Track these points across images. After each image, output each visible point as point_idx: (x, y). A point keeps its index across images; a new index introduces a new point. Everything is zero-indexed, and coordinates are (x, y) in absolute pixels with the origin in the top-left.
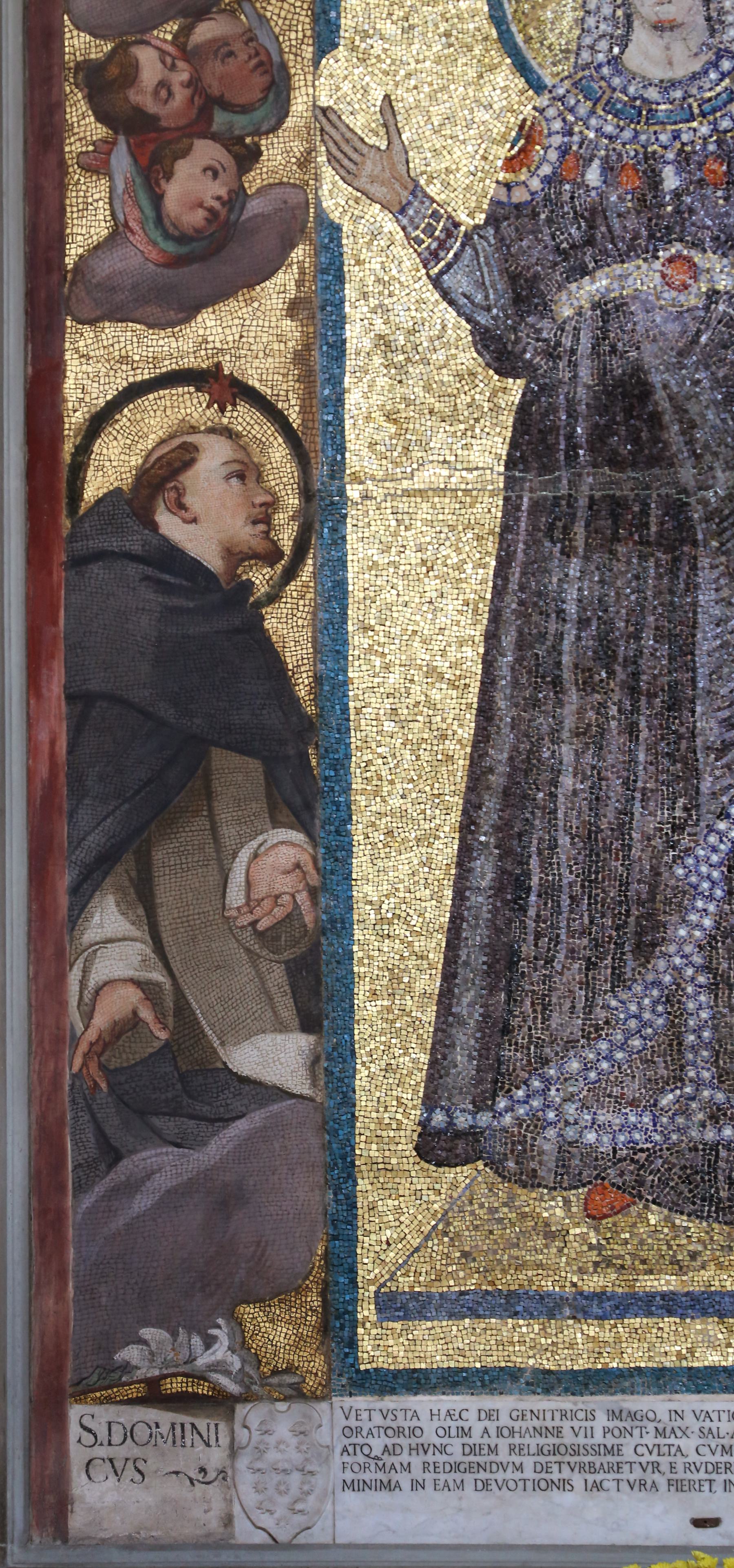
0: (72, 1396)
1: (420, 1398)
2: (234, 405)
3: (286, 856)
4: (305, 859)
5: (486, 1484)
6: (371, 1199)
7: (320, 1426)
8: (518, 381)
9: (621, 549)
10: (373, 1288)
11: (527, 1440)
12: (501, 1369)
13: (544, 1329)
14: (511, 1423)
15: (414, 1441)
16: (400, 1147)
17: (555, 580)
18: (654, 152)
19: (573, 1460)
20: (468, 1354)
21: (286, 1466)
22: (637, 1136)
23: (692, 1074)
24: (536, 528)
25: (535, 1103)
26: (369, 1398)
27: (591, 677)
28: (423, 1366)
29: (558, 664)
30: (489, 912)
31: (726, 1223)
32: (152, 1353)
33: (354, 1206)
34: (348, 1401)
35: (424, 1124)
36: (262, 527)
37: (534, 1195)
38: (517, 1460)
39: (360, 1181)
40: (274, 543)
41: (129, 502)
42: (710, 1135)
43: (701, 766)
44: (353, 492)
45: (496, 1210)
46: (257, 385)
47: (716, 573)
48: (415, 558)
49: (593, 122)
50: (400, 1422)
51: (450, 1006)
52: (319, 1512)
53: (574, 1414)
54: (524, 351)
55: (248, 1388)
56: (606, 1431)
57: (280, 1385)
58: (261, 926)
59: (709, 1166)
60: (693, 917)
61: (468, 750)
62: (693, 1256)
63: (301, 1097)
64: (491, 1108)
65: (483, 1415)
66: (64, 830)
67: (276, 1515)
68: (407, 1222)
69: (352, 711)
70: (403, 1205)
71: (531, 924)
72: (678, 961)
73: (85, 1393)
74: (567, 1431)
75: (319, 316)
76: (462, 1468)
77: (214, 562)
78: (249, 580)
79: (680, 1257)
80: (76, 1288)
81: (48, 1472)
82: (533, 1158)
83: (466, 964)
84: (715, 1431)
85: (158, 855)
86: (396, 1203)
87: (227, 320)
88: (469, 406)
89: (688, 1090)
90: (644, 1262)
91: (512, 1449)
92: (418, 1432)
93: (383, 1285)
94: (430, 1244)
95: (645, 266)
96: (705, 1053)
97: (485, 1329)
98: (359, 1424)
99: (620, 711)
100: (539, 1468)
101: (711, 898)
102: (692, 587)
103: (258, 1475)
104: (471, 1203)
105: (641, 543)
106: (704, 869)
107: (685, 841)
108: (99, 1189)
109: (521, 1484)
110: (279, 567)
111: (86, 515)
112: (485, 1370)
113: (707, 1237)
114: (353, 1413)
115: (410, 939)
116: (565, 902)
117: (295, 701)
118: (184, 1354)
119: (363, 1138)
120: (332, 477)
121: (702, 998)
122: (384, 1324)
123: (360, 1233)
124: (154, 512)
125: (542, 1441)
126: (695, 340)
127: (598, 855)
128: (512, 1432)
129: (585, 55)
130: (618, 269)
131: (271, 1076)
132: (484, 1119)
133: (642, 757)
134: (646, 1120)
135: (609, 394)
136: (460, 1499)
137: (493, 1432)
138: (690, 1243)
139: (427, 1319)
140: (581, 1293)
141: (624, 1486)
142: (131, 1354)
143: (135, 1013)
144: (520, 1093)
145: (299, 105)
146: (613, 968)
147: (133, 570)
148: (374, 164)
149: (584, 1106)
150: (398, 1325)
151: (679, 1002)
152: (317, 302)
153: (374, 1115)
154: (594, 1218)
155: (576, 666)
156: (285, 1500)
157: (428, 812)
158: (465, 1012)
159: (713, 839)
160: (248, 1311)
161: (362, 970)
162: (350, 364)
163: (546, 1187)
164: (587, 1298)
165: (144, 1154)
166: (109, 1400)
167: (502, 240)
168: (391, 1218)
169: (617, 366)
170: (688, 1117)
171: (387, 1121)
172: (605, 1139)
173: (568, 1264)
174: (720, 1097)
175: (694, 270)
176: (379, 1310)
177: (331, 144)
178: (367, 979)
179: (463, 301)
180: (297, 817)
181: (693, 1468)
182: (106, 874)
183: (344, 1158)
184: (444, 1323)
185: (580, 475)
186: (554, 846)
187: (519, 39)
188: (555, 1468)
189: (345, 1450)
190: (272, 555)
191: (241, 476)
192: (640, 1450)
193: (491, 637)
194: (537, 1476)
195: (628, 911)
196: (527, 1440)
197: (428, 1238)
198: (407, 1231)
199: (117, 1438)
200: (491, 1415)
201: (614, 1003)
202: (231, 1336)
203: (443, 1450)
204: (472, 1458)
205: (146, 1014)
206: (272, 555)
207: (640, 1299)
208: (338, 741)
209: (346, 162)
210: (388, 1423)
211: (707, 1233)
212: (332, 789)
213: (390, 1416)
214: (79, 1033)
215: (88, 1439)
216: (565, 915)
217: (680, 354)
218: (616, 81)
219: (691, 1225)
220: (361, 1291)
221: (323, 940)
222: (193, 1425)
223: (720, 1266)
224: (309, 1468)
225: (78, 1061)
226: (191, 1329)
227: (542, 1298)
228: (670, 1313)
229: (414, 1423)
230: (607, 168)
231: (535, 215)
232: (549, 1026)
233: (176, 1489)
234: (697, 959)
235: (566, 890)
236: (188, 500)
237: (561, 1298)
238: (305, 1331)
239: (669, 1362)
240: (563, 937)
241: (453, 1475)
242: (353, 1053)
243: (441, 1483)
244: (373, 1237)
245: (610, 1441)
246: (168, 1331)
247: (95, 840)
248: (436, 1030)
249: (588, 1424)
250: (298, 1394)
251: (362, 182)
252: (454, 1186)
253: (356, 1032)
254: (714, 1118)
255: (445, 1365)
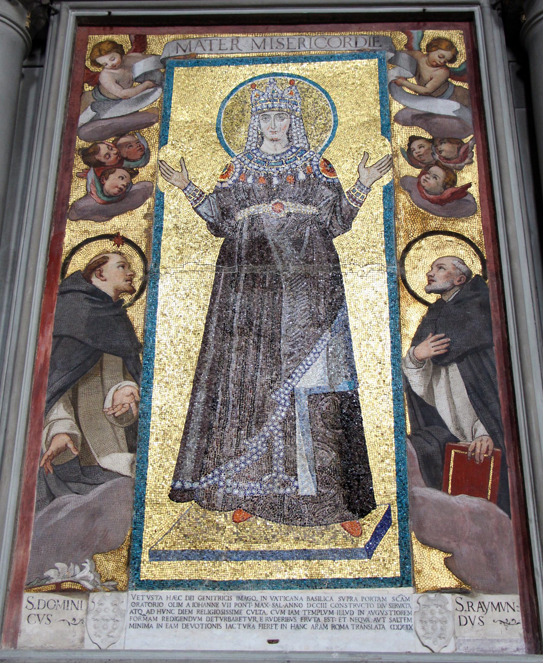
0: (26, 589)
1: (164, 591)
2: (123, 245)
3: (128, 390)
4: (135, 392)
5: (187, 626)
6: (150, 514)
7: (123, 602)
8: (222, 239)
9: (256, 290)
10: (148, 548)
11: (204, 608)
12: (196, 580)
13: (214, 564)
14: (198, 601)
15: (159, 608)
16: (163, 495)
17: (232, 300)
18: (270, 174)
19: (222, 616)
20: (184, 574)
21: (108, 618)
22: (254, 492)
23: (275, 469)
24: (226, 283)
25: (216, 479)
26: (143, 591)
27: (244, 331)
28: (166, 579)
29: (232, 327)
30: (202, 410)
31: (286, 524)
32: (59, 573)
33: (143, 517)
34: (135, 592)
35: (172, 487)
36: (129, 282)
37: (213, 513)
38: (200, 616)
39: (146, 507)
40: (133, 287)
41: (83, 275)
42: (282, 491)
43: (282, 360)
44: (162, 271)
45: (198, 519)
46: (131, 239)
47: (289, 298)
48: (183, 293)
49: (250, 165)
50: (155, 601)
51: (185, 444)
52: (119, 637)
53: (224, 598)
54: (225, 229)
55: (96, 587)
56: (236, 605)
57: (108, 586)
58: (116, 415)
59: (281, 503)
60: (278, 413)
61: (198, 355)
62: (274, 537)
63: (126, 476)
64: (199, 481)
65: (188, 598)
66: (47, 381)
67: (102, 638)
68: (164, 523)
69: (156, 342)
70: (162, 517)
71: (218, 415)
72: (272, 428)
73: (31, 588)
74: (220, 605)
75: (154, 219)
76: (178, 619)
77: (110, 292)
78: (123, 299)
79: (268, 537)
80: (32, 547)
81: (12, 620)
82: (214, 499)
83: (192, 428)
84: (278, 605)
85: (81, 390)
86: (160, 516)
87: (123, 220)
88: (204, 245)
89: (274, 474)
90: (254, 539)
91: (198, 611)
92: (161, 605)
93: (152, 547)
94: (172, 531)
95: (266, 205)
96: (281, 461)
97: (191, 565)
98: (138, 601)
99: (253, 342)
100: (208, 619)
101: (285, 406)
102: (280, 301)
103: (96, 621)
104: (189, 516)
105: (263, 288)
106: (282, 396)
107: (276, 386)
108: (46, 510)
109: (201, 626)
110: (134, 295)
111: (67, 278)
112: (190, 581)
113: (279, 530)
114: (136, 597)
115: (172, 420)
116: (231, 407)
117: (136, 338)
118: (72, 573)
119: (149, 492)
120: (155, 267)
121: (280, 441)
122: (152, 562)
123: (145, 527)
124: (91, 278)
125: (210, 608)
126: (283, 226)
127: (243, 391)
128: (199, 605)
129: (248, 147)
130: (257, 206)
131: (115, 468)
132: (196, 485)
133: (261, 357)
134: (257, 485)
135: (253, 243)
136: (176, 631)
137: (191, 605)
138: (272, 531)
139: (168, 560)
140: (229, 551)
141: (242, 626)
142: (51, 573)
143: (66, 445)
144: (210, 475)
145: (153, 160)
146: (248, 430)
147: (82, 296)
148: (177, 176)
149: (234, 480)
150: (157, 563)
151: (272, 443)
152: (154, 214)
153: (154, 483)
154: (236, 522)
155: (238, 327)
156: (106, 632)
157: (182, 376)
158: (191, 446)
159: (286, 385)
160: (98, 557)
161: (153, 430)
162: (164, 232)
163: (218, 510)
164: (231, 553)
165: (64, 497)
166: (40, 591)
167: (218, 198)
168: (157, 521)
169: (256, 235)
170: (274, 485)
171: (158, 485)
172: (242, 492)
173: (225, 540)
174: (286, 477)
175: (283, 206)
176: (150, 557)
177: (162, 170)
178: (155, 434)
179: (204, 214)
180: (133, 377)
181: (269, 619)
182: (61, 396)
183: (141, 499)
184: (175, 562)
185: (242, 267)
186: (227, 388)
187: (227, 143)
188: (215, 619)
189: (132, 612)
190: (132, 291)
191: (123, 267)
192: (249, 612)
193: (208, 318)
194: (207, 623)
195: (254, 410)
196: (204, 608)
197: (171, 529)
198: (163, 526)
199: (41, 606)
200: (190, 598)
201: (247, 443)
202: (91, 566)
203: (170, 612)
204: (182, 615)
205: (70, 446)
206: (132, 291)
207: (252, 553)
208: (150, 352)
209: (167, 175)
210: (150, 601)
211: (279, 528)
212: (147, 367)
213: (151, 598)
214: (44, 452)
215: (30, 606)
216: (230, 411)
217: (278, 231)
218: (258, 154)
219: (273, 525)
220: (143, 549)
221: (139, 420)
222: (72, 601)
223: (284, 540)
224: (117, 619)
225: (43, 462)
226: (75, 563)
227: (214, 552)
228: (264, 558)
229: (160, 601)
230: (255, 178)
231: (230, 191)
232: (222, 451)
233: (63, 626)
234: (279, 427)
235: (231, 403)
236: (103, 274)
237: (222, 553)
238: (120, 564)
239: (262, 577)
240: (229, 419)
241: (174, 622)
242: (147, 460)
243: (169, 625)
244: (150, 529)
245: (237, 608)
246: (66, 564)
247: (58, 385)
248: (180, 452)
249: (229, 602)
250: (116, 589)
251: (173, 181)
252: (182, 509)
253: (149, 453)
254: (284, 485)
255: (174, 579)
